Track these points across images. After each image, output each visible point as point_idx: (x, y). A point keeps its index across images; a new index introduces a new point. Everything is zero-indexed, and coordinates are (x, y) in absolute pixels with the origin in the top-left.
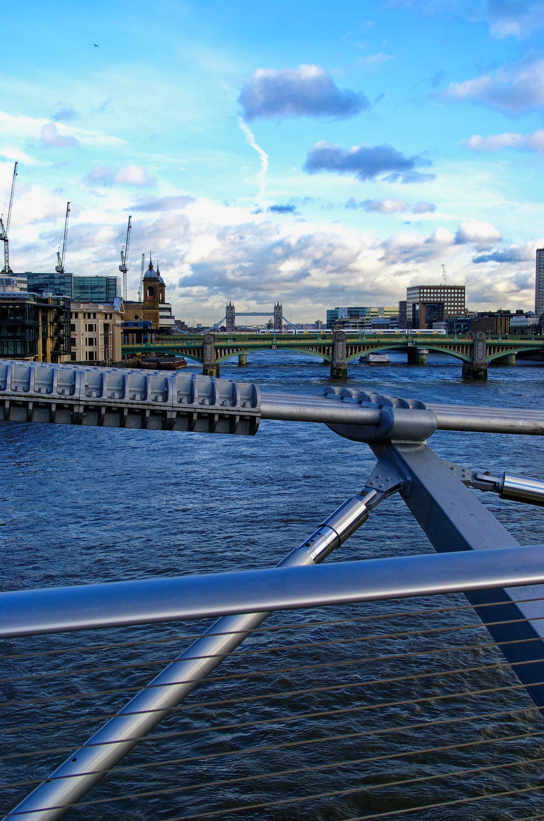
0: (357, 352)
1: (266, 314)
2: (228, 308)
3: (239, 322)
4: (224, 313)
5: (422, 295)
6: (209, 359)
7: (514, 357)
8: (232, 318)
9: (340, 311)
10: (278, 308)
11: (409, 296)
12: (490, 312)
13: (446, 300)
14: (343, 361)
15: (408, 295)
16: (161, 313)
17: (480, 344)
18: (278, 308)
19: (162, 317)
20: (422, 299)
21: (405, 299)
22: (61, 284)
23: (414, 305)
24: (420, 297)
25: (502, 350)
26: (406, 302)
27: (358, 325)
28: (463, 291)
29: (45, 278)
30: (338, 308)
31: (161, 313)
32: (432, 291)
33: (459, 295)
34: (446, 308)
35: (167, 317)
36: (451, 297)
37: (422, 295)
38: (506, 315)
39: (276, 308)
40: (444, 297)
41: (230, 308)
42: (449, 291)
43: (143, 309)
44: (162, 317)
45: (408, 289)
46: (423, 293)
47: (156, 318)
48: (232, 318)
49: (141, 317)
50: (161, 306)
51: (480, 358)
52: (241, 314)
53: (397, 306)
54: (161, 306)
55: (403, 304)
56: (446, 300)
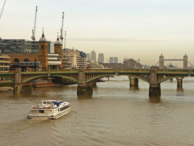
0: (91, 78)
2: (160, 57)
3: (166, 64)
4: (158, 60)
6: (17, 80)
8: (162, 62)
10: (186, 57)
14: (82, 82)
16: (49, 58)
17: (153, 74)
18: (186, 57)
19: (49, 60)
22: (20, 45)
29: (13, 42)
31: (49, 58)
35: (56, 60)
39: (184, 57)
41: (161, 57)
43: (38, 56)
44: (49, 60)
47: (44, 61)
48: (162, 62)
49: (37, 60)
50: (49, 55)
51: (153, 81)
52: (167, 60)
54: (49, 55)
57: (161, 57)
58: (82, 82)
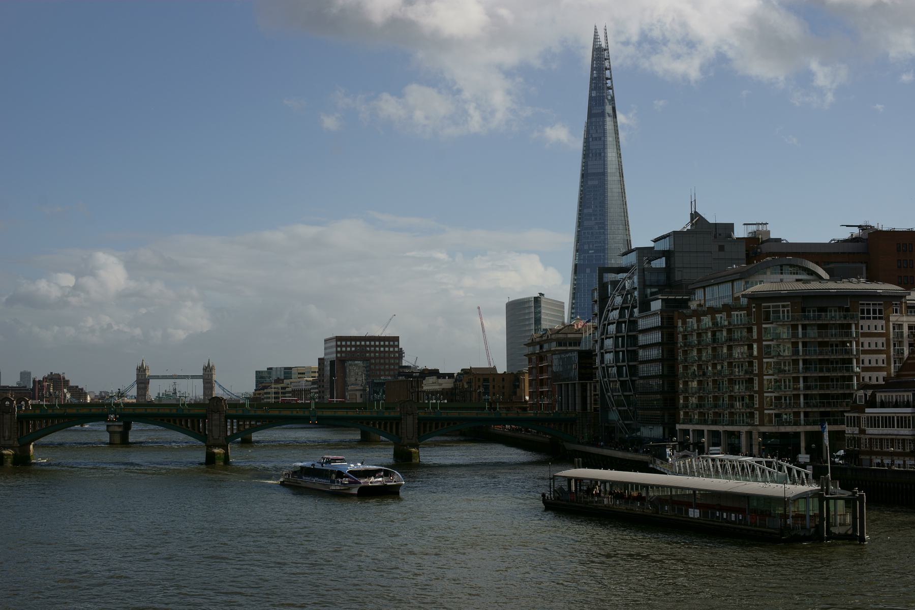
1: (193, 377)
5: (339, 349)
9: (274, 373)
10: (208, 370)
11: (328, 351)
13: (372, 355)
15: (325, 349)
18: (208, 370)
20: (339, 355)
21: (322, 356)
24: (337, 352)
27: (280, 391)
28: (396, 343)
32: (349, 343)
33: (391, 349)
37: (339, 349)
38: (435, 373)
41: (141, 370)
42: (377, 343)
45: (326, 341)
46: (341, 346)
52: (157, 377)
53: (315, 365)
55: (321, 361)
56: (372, 355)
57: (141, 370)
58: (11, 442)
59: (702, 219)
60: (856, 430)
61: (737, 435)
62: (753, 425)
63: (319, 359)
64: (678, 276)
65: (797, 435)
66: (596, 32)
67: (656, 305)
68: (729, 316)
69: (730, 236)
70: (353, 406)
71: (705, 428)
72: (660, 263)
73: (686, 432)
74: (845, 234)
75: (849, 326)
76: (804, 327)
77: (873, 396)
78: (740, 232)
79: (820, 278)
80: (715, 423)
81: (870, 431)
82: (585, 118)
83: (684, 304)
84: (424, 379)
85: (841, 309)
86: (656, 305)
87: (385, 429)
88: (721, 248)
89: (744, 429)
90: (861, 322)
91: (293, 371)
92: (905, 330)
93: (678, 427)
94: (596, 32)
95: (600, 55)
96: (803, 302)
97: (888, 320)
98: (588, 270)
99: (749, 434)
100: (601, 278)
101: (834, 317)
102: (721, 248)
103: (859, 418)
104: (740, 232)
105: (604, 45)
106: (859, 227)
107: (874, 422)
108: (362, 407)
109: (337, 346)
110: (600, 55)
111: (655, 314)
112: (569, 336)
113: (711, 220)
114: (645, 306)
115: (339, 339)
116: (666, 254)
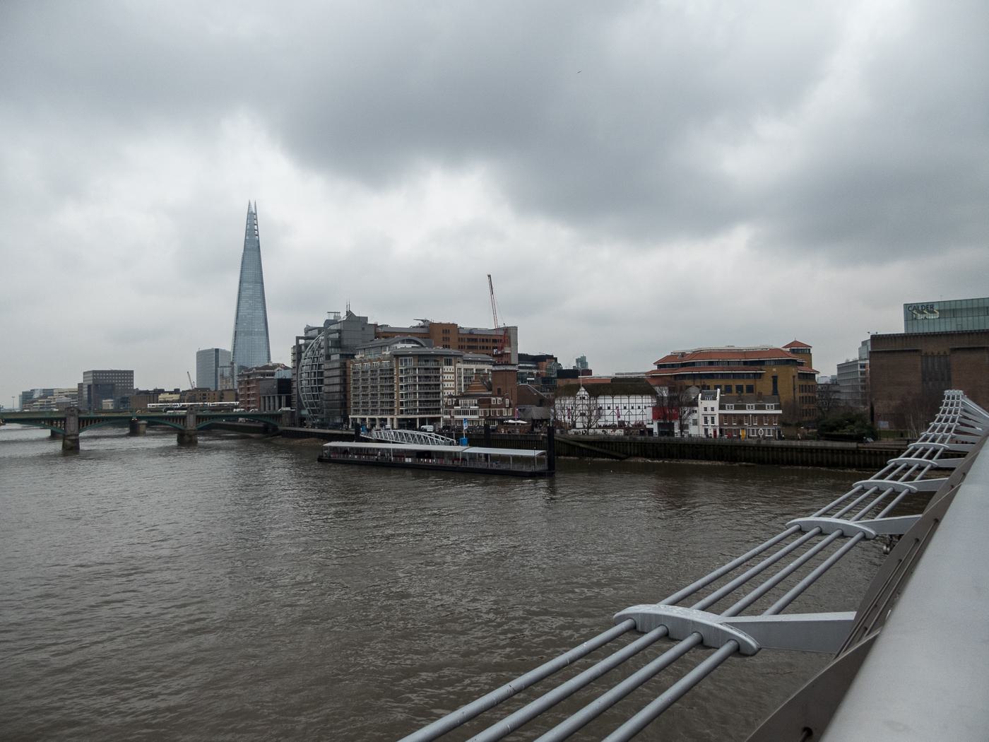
7: (144, 426)
12: (148, 391)
17: (72, 418)
23: (89, 386)
24: (93, 380)
25: (99, 421)
26: (82, 384)
30: (33, 390)
34: (117, 388)
36: (121, 380)
40: (115, 380)
45: (84, 373)
46: (96, 376)
53: (76, 387)
55: (80, 385)
59: (352, 314)
60: (448, 417)
61: (385, 420)
62: (393, 414)
63: (79, 384)
64: (345, 343)
65: (416, 419)
66: (250, 204)
67: (335, 357)
68: (381, 363)
69: (366, 324)
70: (107, 411)
71: (367, 417)
72: (337, 336)
73: (355, 419)
74: (416, 324)
75: (439, 369)
76: (419, 369)
77: (457, 401)
78: (370, 322)
79: (422, 346)
80: (372, 414)
81: (457, 417)
82: (243, 251)
83: (353, 356)
84: (160, 394)
85: (435, 361)
86: (335, 357)
87: (180, 423)
88: (363, 329)
89: (389, 417)
90: (444, 367)
91: (55, 391)
92: (462, 370)
93: (350, 417)
94: (250, 204)
95: (252, 217)
96: (420, 357)
97: (455, 367)
98: (242, 334)
99: (392, 419)
100: (297, 341)
101: (431, 365)
102: (363, 329)
103: (450, 411)
104: (370, 322)
105: (254, 212)
106: (422, 320)
107: (458, 413)
108: (113, 411)
109: (93, 376)
110: (252, 217)
111: (336, 361)
112: (268, 371)
113: (357, 315)
114: (328, 357)
115: (94, 372)
116: (339, 331)
